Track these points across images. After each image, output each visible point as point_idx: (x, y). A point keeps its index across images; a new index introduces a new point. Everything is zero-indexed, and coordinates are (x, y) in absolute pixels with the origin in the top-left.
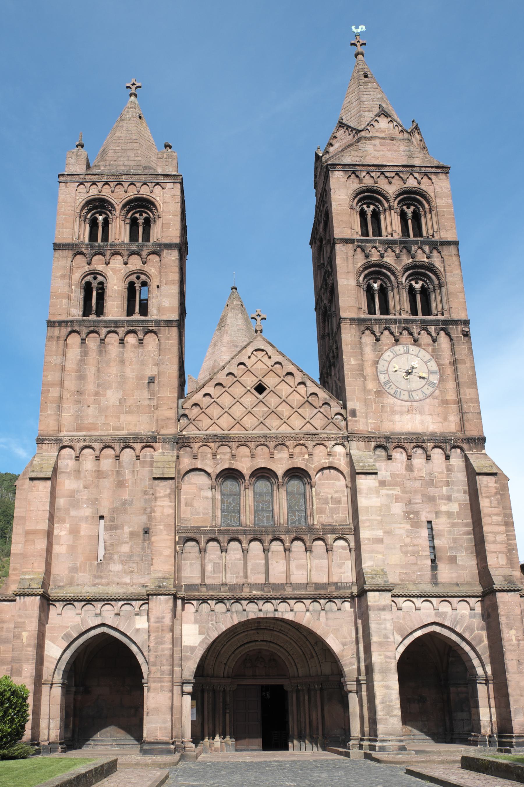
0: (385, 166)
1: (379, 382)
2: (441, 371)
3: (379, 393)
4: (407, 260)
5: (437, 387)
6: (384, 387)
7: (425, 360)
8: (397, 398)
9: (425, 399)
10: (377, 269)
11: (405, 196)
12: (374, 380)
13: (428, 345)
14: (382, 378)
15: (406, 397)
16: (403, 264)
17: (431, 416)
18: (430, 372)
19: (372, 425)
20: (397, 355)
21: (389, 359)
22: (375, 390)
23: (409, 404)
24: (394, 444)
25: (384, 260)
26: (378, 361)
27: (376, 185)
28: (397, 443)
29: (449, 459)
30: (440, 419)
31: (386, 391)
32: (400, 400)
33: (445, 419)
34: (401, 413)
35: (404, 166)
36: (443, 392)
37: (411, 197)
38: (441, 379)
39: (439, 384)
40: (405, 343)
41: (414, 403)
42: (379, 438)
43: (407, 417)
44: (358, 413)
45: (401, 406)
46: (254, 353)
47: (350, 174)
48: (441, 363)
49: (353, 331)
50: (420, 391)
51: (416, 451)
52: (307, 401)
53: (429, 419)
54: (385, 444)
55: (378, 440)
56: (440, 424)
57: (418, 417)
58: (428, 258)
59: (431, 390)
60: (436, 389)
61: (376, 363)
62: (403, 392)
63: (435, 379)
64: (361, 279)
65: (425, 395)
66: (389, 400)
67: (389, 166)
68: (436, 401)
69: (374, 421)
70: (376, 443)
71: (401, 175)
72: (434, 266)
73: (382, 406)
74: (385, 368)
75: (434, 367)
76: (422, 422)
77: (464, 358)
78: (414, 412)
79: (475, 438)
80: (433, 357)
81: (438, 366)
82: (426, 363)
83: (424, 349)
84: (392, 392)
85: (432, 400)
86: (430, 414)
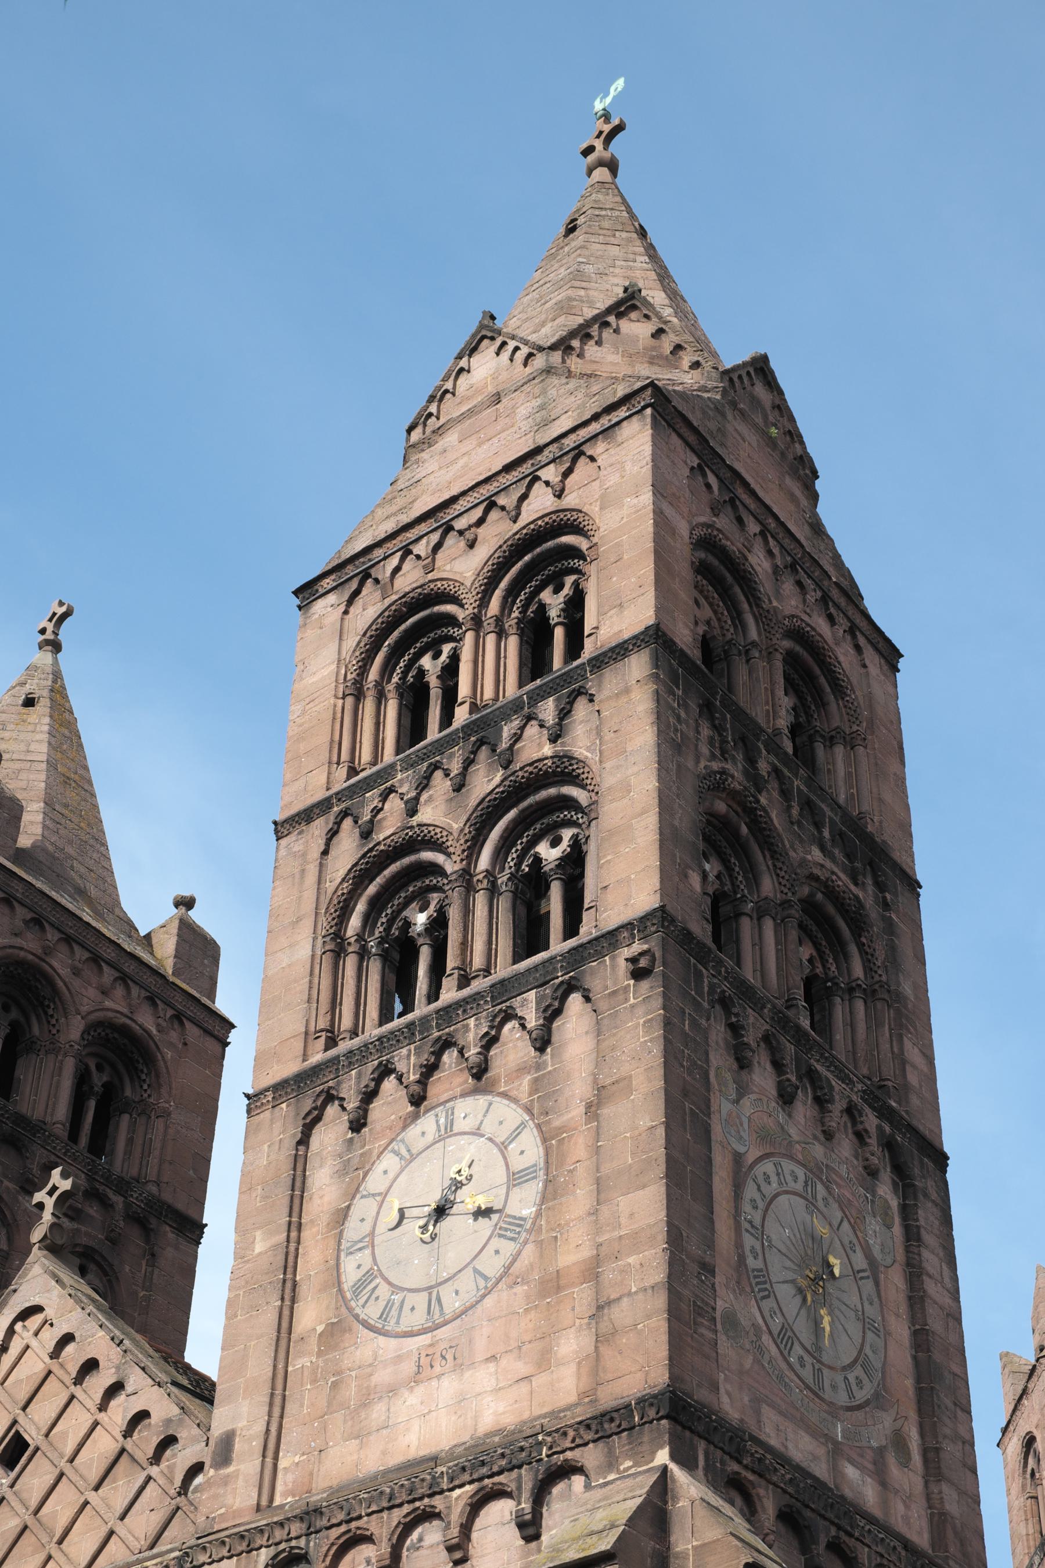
0: (454, 500)
1: (340, 1291)
2: (553, 1159)
3: (334, 1334)
4: (485, 781)
5: (529, 1232)
6: (353, 1304)
7: (499, 1140)
8: (385, 1334)
9: (484, 1296)
10: (406, 861)
11: (527, 558)
12: (324, 1288)
13: (522, 1070)
14: (351, 1270)
15: (416, 1319)
16: (473, 802)
17: (492, 1367)
18: (515, 1179)
19: (290, 1477)
20: (413, 1157)
21: (382, 1189)
22: (320, 1329)
23: (424, 1340)
24: (335, 1533)
25: (415, 820)
26: (348, 1207)
27: (430, 576)
28: (343, 1528)
29: (537, 1537)
30: (522, 1368)
31: (356, 1317)
32: (398, 1336)
33: (545, 1360)
34: (392, 1390)
35: (508, 468)
36: (547, 1246)
37: (549, 551)
38: (551, 1193)
39: (539, 1214)
40: (445, 1097)
41: (441, 1333)
42: (281, 1524)
43: (412, 1399)
44: (238, 1446)
45: (398, 1359)
46: (18, 1327)
47: (354, 585)
48: (557, 1123)
49: (278, 1126)
50: (470, 1269)
51: (420, 1539)
52: (123, 1451)
53: (483, 1377)
54: (302, 1542)
55: (279, 1534)
56: (524, 1388)
57: (447, 1387)
58: (554, 739)
59: (508, 1248)
60: (526, 1242)
61: (342, 1216)
62: (412, 1299)
63: (524, 1203)
64: (355, 922)
65: (482, 1283)
66: (365, 1348)
67: (464, 493)
68: (520, 1289)
69: (297, 1459)
70: (272, 1551)
71: (501, 501)
72: (571, 758)
73: (335, 1384)
74: (367, 1227)
75: (529, 1149)
76: (461, 1400)
77: (625, 1069)
78: (437, 1369)
79: (628, 1406)
80: (529, 1110)
81: (544, 1140)
82: (503, 1148)
83: (504, 1095)
84: (372, 1312)
85: (505, 1295)
86: (493, 1358)
